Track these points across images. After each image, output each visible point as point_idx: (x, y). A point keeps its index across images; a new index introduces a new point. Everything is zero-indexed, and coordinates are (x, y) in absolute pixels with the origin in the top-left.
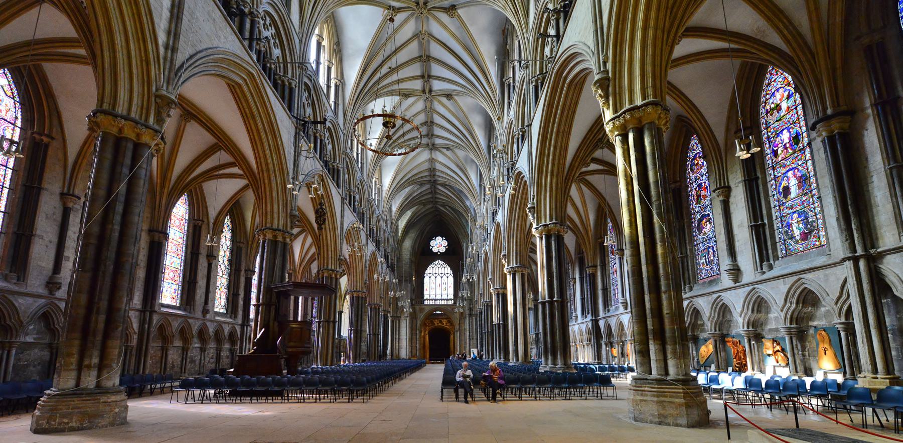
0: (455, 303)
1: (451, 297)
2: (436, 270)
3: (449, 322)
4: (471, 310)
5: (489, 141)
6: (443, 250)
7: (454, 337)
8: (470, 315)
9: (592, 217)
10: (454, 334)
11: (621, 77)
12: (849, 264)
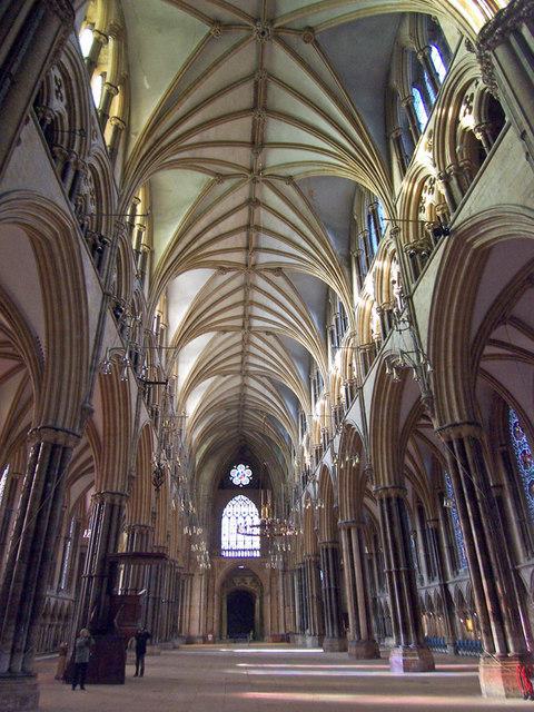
0: (263, 555)
2: (238, 509)
3: (254, 580)
4: (285, 564)
5: (309, 373)
6: (246, 481)
7: (261, 603)
8: (285, 571)
9: (428, 466)
10: (261, 598)
11: (442, 398)
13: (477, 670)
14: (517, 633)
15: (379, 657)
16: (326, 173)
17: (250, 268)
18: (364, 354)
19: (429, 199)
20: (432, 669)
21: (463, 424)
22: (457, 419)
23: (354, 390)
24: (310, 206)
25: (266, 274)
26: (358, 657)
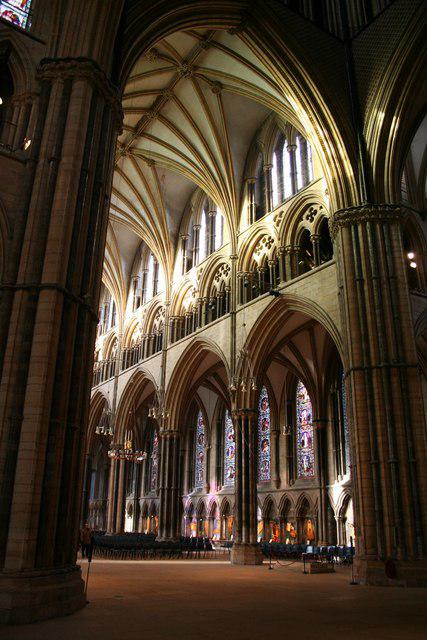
12: (318, 491)
18: (173, 323)
19: (266, 251)
22: (248, 407)
24: (159, 188)
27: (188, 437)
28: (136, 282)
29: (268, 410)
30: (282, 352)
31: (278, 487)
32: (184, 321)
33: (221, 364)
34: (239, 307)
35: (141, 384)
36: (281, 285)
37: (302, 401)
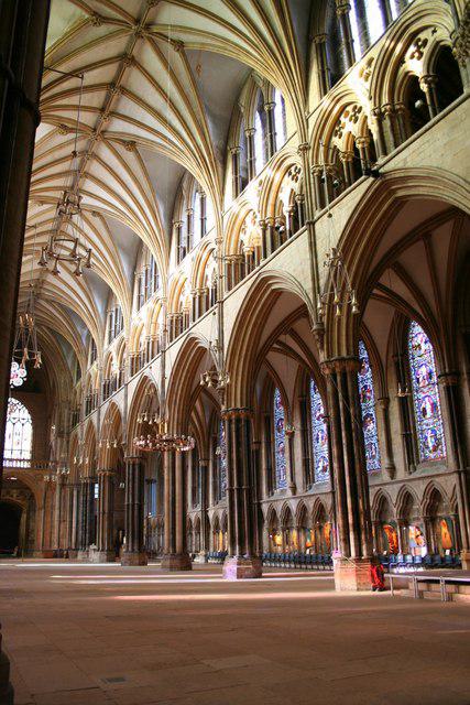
1: (28, 456)
3: (21, 493)
8: (63, 485)
12: (456, 475)
13: (333, 575)
14: (369, 543)
15: (191, 569)
16: (221, 52)
17: (98, 133)
18: (229, 265)
19: (350, 127)
20: (260, 577)
21: (349, 359)
22: (344, 354)
23: (208, 301)
24: (194, 83)
25: (113, 143)
26: (172, 568)
27: (263, 425)
28: (179, 229)
29: (369, 375)
30: (384, 280)
31: (392, 477)
32: (244, 260)
33: (302, 311)
34: (317, 214)
35: (194, 355)
36: (380, 161)
37: (416, 353)
